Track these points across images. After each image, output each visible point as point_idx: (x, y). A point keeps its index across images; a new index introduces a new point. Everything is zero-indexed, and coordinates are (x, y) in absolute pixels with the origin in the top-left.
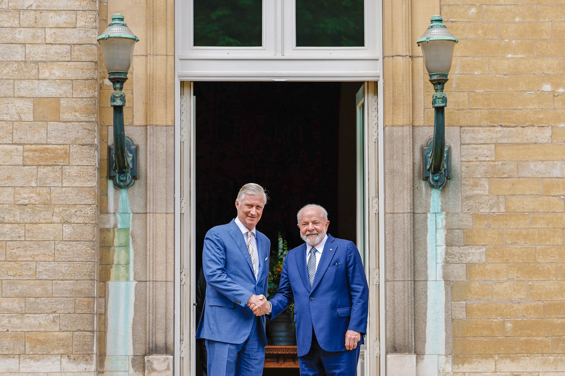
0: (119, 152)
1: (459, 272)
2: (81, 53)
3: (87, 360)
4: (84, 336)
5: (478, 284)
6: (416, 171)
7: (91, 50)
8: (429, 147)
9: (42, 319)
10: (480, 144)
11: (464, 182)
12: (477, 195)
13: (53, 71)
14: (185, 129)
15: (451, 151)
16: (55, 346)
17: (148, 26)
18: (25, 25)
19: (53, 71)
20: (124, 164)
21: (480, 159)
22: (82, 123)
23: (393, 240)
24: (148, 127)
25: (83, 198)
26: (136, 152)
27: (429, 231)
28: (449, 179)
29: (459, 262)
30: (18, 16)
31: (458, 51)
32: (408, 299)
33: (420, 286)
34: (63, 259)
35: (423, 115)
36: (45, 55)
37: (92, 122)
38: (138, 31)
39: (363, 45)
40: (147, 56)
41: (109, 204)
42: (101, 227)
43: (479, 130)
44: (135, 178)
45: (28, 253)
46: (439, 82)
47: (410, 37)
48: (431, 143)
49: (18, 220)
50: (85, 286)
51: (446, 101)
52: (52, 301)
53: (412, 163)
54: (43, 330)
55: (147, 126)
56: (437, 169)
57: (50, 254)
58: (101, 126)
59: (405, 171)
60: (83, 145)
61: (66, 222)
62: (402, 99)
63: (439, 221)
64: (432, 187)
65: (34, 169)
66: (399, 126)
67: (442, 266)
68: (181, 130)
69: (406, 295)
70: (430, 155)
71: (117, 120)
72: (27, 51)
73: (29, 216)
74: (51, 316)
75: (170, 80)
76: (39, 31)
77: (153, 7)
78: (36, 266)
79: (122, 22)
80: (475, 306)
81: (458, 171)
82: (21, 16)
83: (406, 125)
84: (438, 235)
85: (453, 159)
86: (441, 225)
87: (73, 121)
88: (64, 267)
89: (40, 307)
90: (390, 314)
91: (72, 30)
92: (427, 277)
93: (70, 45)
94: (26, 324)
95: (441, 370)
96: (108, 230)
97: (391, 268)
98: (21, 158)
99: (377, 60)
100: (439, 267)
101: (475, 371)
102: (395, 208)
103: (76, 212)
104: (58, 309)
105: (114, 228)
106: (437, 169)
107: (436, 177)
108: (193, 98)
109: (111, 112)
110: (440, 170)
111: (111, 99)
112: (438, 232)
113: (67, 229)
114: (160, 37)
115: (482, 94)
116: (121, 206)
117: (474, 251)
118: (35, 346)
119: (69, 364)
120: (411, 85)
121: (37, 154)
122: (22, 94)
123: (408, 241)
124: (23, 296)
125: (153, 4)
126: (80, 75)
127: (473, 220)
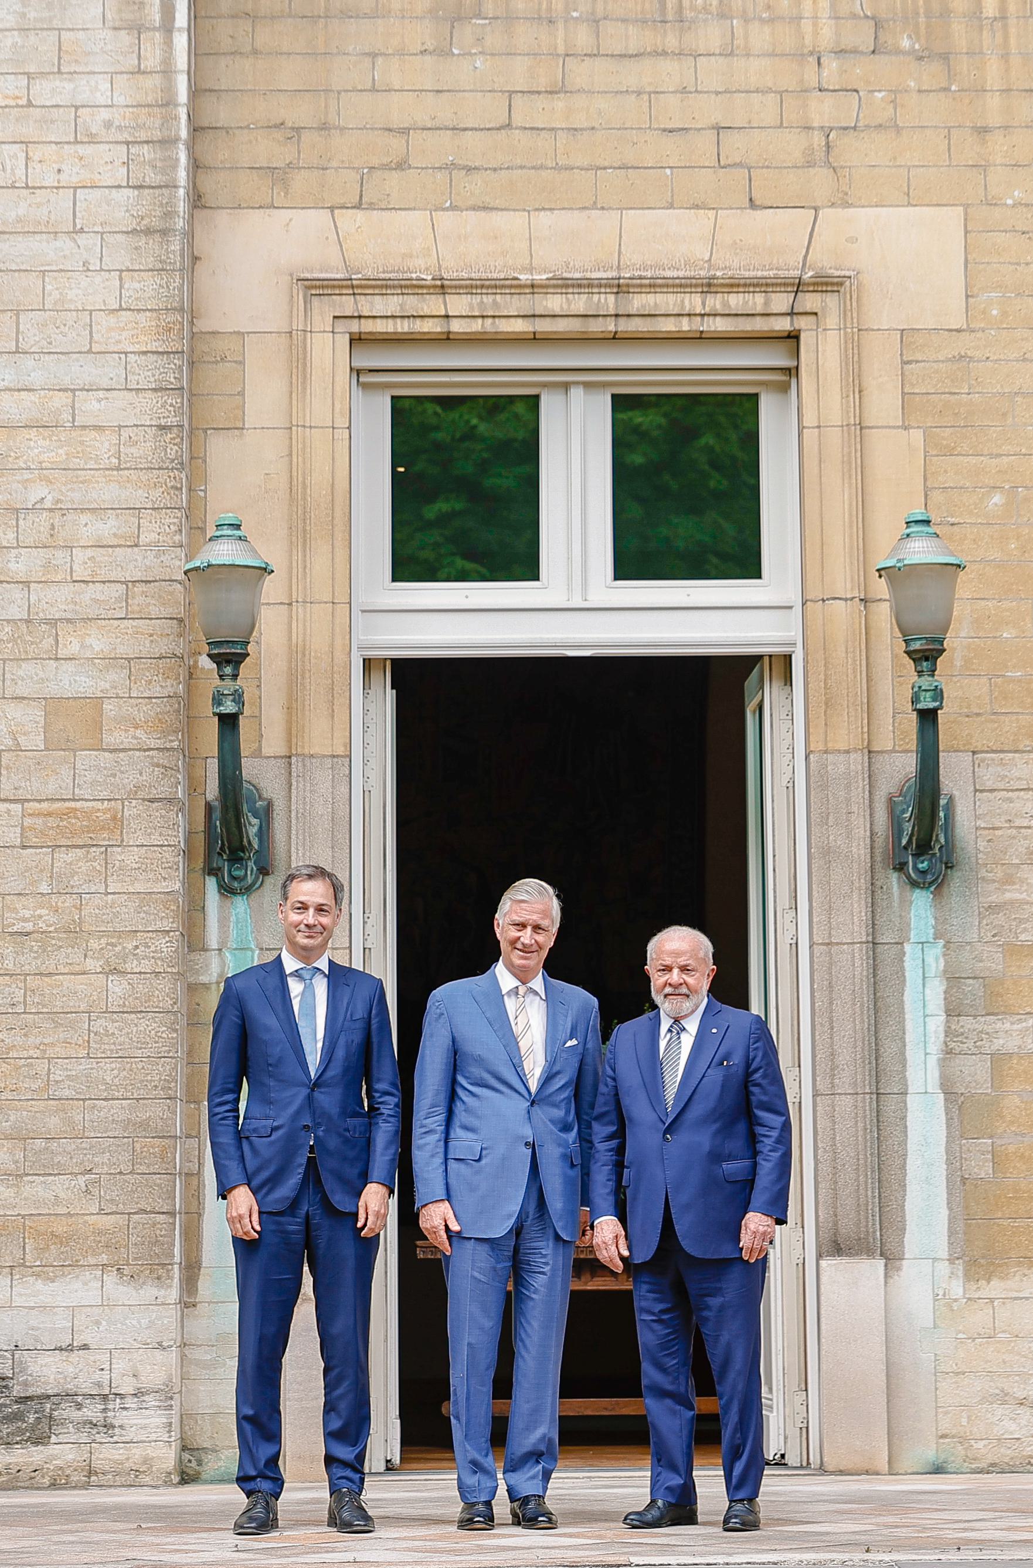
0: (231, 814)
1: (975, 1073)
2: (148, 600)
3: (158, 1278)
4: (154, 1225)
5: (1017, 1100)
6: (878, 852)
7: (171, 593)
8: (905, 797)
9: (61, 1187)
10: (1017, 790)
11: (983, 873)
12: (1012, 902)
13: (88, 641)
14: (373, 764)
15: (954, 807)
16: (90, 1247)
17: (294, 539)
18: (29, 542)
19: (88, 641)
20: (242, 841)
21: (1016, 824)
22: (151, 753)
23: (831, 1003)
24: (294, 759)
25: (152, 917)
26: (266, 814)
27: (908, 984)
28: (951, 867)
29: (974, 1050)
30: (14, 523)
31: (965, 587)
32: (865, 1134)
33: (890, 1105)
34: (109, 1054)
35: (891, 728)
36: (71, 606)
37: (172, 749)
38: (272, 553)
39: (760, 577)
40: (290, 604)
41: (207, 929)
42: (191, 980)
43: (1014, 758)
44: (264, 871)
45: (31, 1040)
46: (926, 656)
47: (861, 558)
48: (909, 787)
49: (11, 966)
50: (155, 1111)
51: (942, 698)
52: (84, 1145)
53: (868, 833)
54: (65, 1211)
55: (290, 757)
56: (923, 847)
57: (80, 1042)
58: (191, 757)
59: (854, 850)
60: (151, 801)
61: (115, 971)
62: (845, 692)
63: (930, 960)
64: (914, 884)
65: (45, 854)
66: (839, 751)
67: (939, 1059)
68: (364, 764)
69: (860, 1125)
70: (908, 815)
71: (226, 745)
72: (33, 598)
73: (35, 958)
74: (82, 1180)
75: (340, 657)
76: (59, 554)
77: (304, 499)
78: (49, 1070)
79: (237, 533)
80: (1011, 1148)
81: (971, 849)
82: (21, 522)
83: (856, 750)
84: (928, 991)
85: (958, 824)
86: (933, 969)
87: (130, 750)
88: (109, 1072)
89: (56, 1161)
90: (825, 1168)
91: (130, 549)
92: (906, 1085)
93: (125, 583)
94: (25, 1199)
95: (941, 1293)
96: (206, 986)
97: (827, 1065)
98: (18, 830)
99: (791, 607)
100: (933, 1061)
101: (1016, 1295)
102: (833, 932)
103: (137, 947)
104: (97, 1165)
105: (218, 983)
106: (923, 847)
107: (922, 862)
108: (391, 695)
109: (211, 729)
110: (931, 849)
111: (213, 699)
112: (927, 985)
113: (117, 987)
114: (320, 563)
115: (1020, 681)
116: (233, 933)
117: (1007, 1026)
118: (47, 1248)
119: (121, 1287)
120: (864, 663)
121: (52, 822)
122: (22, 690)
123: (862, 1005)
124: (20, 1137)
125: (304, 493)
126: (146, 648)
127: (1004, 957)
